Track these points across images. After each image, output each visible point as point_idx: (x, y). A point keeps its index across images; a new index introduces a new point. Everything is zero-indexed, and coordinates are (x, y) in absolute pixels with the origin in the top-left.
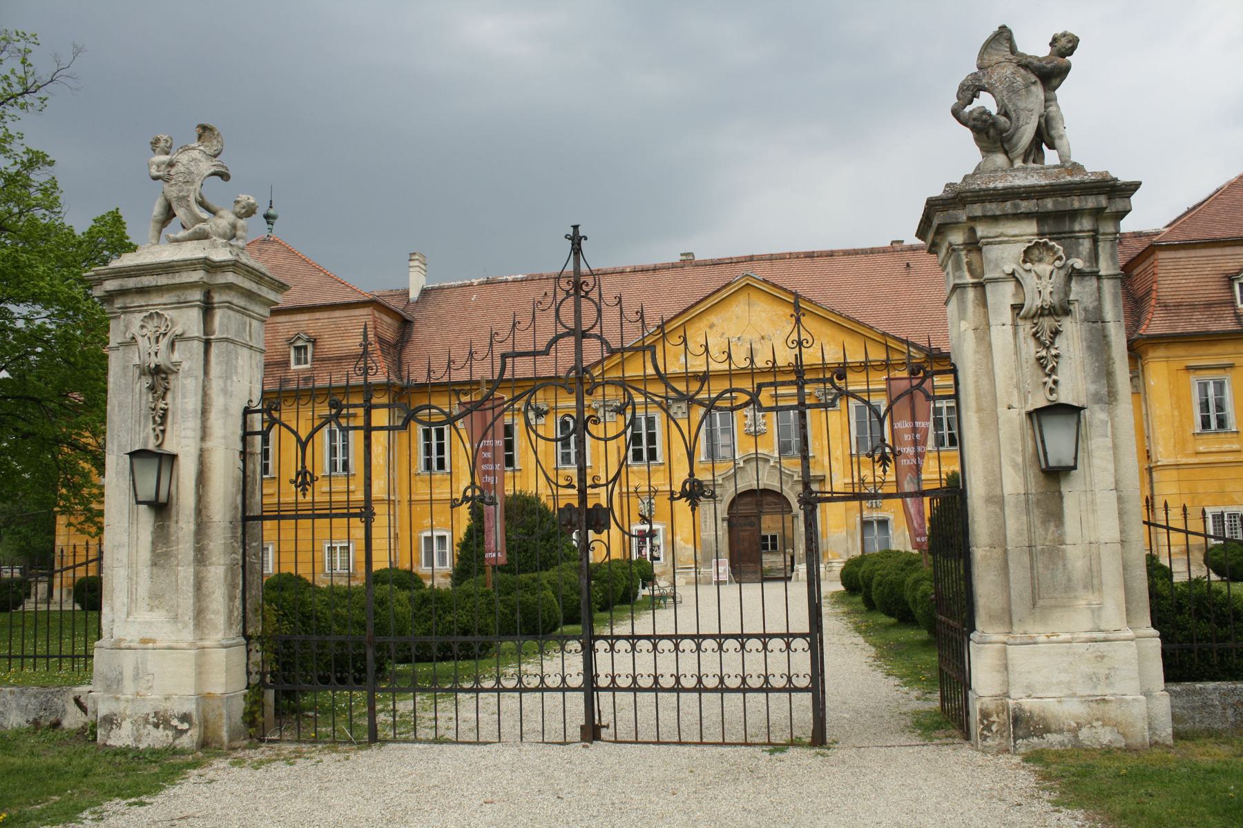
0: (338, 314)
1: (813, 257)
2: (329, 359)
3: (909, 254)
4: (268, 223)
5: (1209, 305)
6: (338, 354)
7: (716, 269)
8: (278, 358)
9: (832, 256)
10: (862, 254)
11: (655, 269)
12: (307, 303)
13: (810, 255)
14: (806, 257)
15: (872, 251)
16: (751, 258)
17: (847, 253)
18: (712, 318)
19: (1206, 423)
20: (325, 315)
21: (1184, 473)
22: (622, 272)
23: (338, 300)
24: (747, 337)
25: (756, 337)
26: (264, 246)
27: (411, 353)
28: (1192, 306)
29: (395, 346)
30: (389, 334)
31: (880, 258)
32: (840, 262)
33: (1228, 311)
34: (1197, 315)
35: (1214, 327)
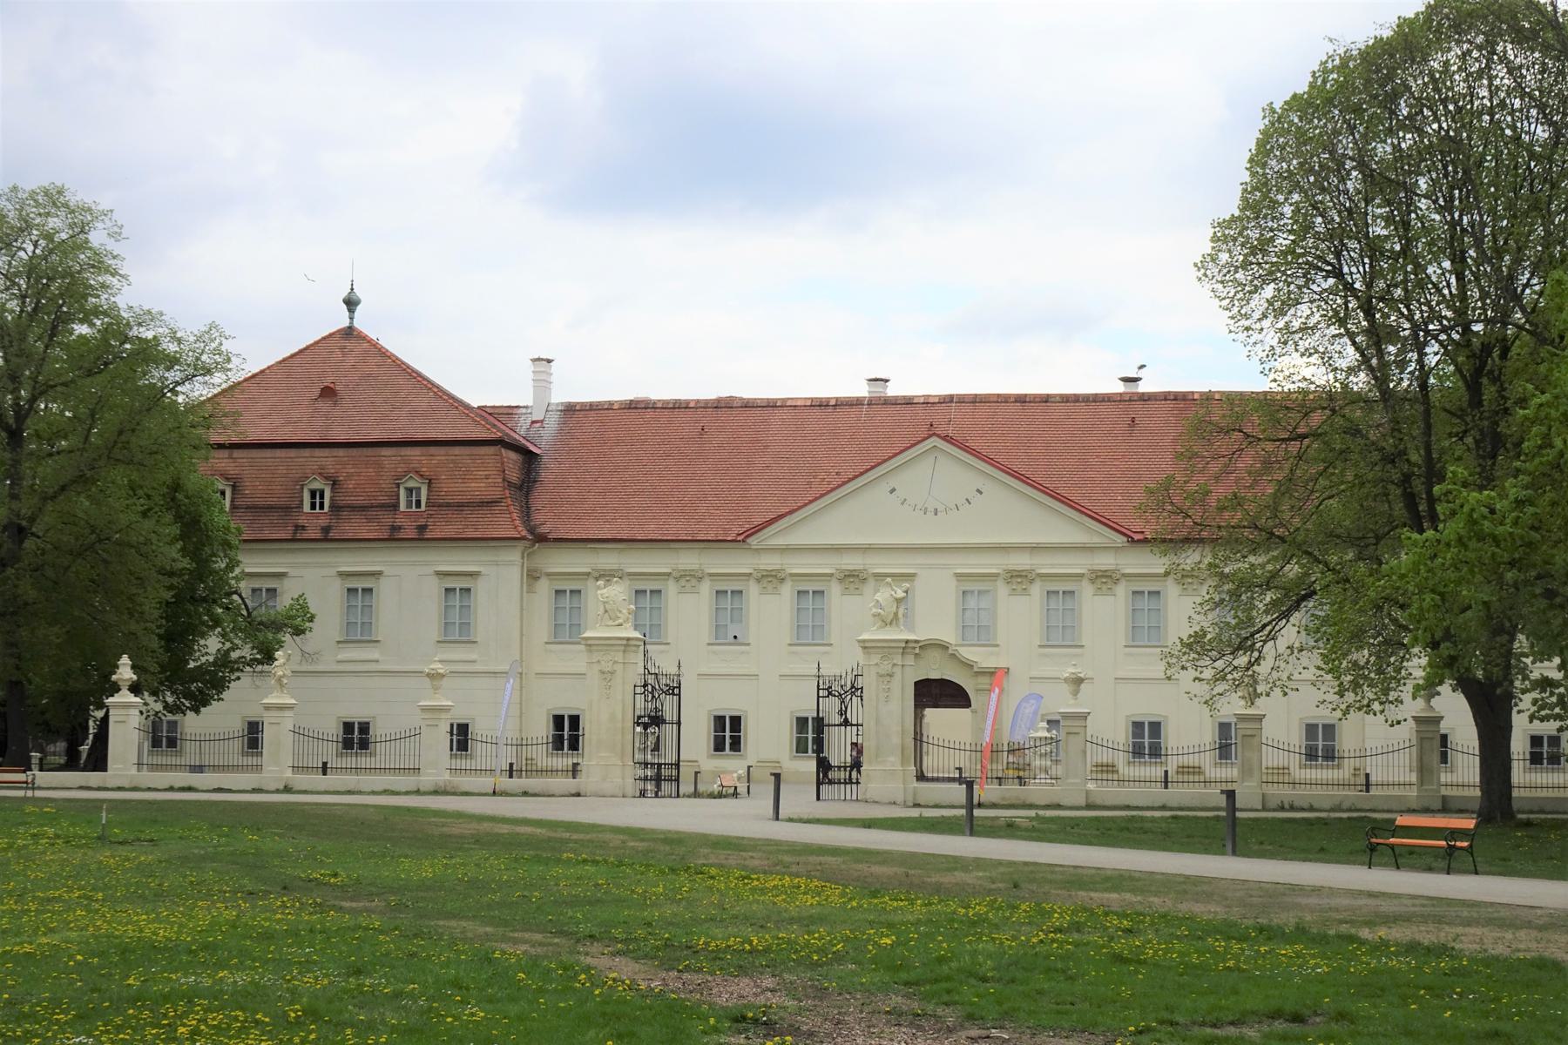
0: (457, 450)
1: (1025, 402)
2: (448, 505)
4: (349, 310)
6: (458, 499)
8: (383, 500)
9: (1046, 402)
10: (1083, 401)
12: (420, 436)
14: (1016, 401)
20: (442, 450)
23: (460, 436)
26: (347, 343)
27: (540, 498)
29: (520, 488)
30: (514, 476)
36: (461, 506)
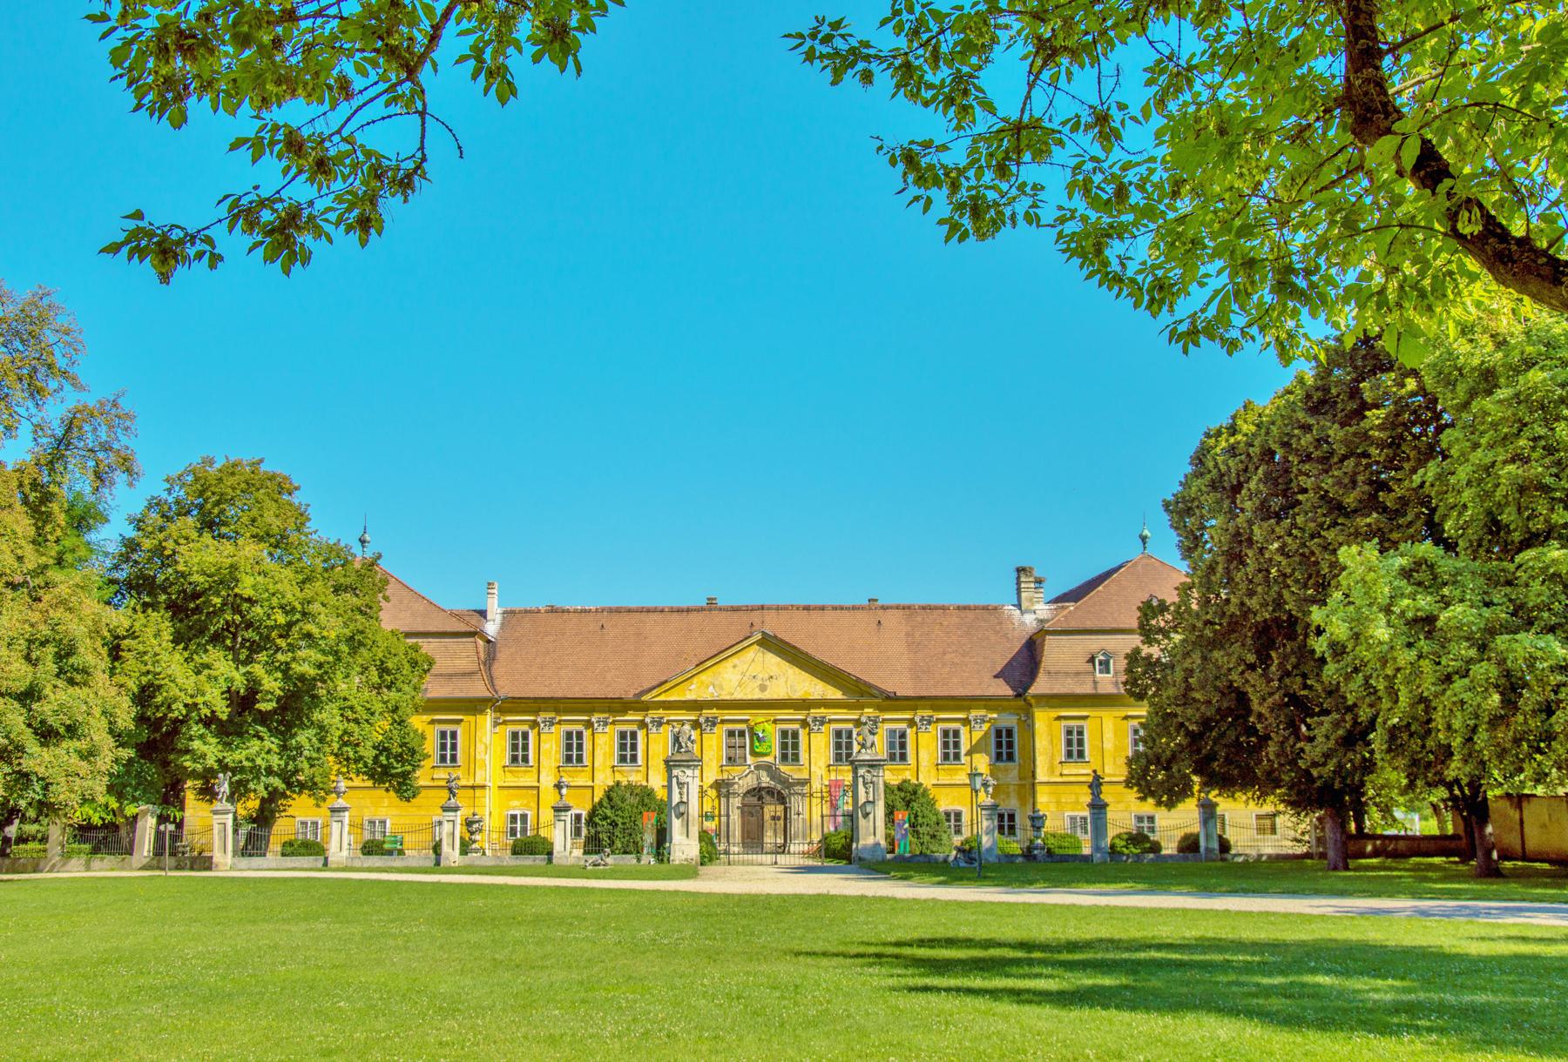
3: (880, 612)
5: (1078, 674)
6: (450, 671)
7: (736, 615)
11: (688, 610)
13: (807, 608)
15: (854, 608)
16: (762, 608)
17: (835, 608)
18: (734, 660)
19: (1069, 754)
21: (1054, 787)
22: (662, 611)
24: (760, 676)
25: (767, 676)
27: (499, 669)
28: (1067, 673)
31: (859, 614)
32: (829, 614)
33: (1089, 679)
34: (1069, 680)
35: (1079, 690)
36: (451, 675)
